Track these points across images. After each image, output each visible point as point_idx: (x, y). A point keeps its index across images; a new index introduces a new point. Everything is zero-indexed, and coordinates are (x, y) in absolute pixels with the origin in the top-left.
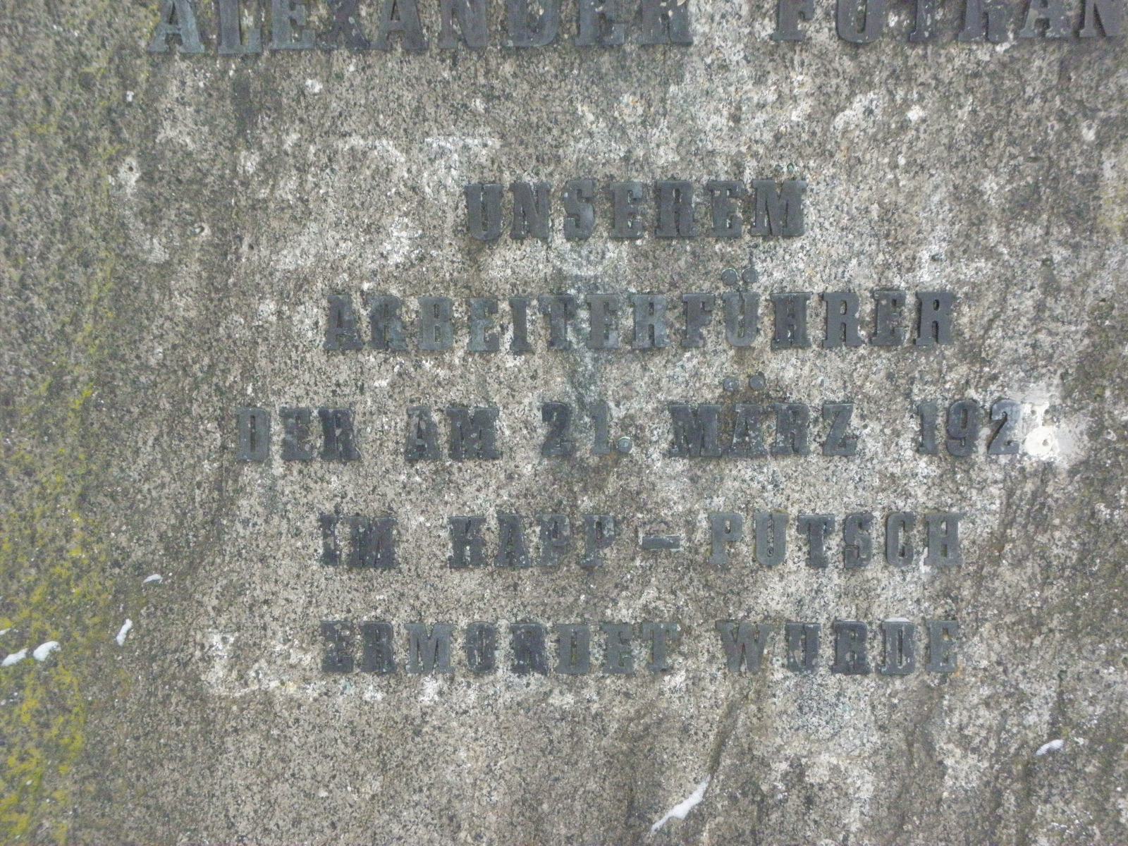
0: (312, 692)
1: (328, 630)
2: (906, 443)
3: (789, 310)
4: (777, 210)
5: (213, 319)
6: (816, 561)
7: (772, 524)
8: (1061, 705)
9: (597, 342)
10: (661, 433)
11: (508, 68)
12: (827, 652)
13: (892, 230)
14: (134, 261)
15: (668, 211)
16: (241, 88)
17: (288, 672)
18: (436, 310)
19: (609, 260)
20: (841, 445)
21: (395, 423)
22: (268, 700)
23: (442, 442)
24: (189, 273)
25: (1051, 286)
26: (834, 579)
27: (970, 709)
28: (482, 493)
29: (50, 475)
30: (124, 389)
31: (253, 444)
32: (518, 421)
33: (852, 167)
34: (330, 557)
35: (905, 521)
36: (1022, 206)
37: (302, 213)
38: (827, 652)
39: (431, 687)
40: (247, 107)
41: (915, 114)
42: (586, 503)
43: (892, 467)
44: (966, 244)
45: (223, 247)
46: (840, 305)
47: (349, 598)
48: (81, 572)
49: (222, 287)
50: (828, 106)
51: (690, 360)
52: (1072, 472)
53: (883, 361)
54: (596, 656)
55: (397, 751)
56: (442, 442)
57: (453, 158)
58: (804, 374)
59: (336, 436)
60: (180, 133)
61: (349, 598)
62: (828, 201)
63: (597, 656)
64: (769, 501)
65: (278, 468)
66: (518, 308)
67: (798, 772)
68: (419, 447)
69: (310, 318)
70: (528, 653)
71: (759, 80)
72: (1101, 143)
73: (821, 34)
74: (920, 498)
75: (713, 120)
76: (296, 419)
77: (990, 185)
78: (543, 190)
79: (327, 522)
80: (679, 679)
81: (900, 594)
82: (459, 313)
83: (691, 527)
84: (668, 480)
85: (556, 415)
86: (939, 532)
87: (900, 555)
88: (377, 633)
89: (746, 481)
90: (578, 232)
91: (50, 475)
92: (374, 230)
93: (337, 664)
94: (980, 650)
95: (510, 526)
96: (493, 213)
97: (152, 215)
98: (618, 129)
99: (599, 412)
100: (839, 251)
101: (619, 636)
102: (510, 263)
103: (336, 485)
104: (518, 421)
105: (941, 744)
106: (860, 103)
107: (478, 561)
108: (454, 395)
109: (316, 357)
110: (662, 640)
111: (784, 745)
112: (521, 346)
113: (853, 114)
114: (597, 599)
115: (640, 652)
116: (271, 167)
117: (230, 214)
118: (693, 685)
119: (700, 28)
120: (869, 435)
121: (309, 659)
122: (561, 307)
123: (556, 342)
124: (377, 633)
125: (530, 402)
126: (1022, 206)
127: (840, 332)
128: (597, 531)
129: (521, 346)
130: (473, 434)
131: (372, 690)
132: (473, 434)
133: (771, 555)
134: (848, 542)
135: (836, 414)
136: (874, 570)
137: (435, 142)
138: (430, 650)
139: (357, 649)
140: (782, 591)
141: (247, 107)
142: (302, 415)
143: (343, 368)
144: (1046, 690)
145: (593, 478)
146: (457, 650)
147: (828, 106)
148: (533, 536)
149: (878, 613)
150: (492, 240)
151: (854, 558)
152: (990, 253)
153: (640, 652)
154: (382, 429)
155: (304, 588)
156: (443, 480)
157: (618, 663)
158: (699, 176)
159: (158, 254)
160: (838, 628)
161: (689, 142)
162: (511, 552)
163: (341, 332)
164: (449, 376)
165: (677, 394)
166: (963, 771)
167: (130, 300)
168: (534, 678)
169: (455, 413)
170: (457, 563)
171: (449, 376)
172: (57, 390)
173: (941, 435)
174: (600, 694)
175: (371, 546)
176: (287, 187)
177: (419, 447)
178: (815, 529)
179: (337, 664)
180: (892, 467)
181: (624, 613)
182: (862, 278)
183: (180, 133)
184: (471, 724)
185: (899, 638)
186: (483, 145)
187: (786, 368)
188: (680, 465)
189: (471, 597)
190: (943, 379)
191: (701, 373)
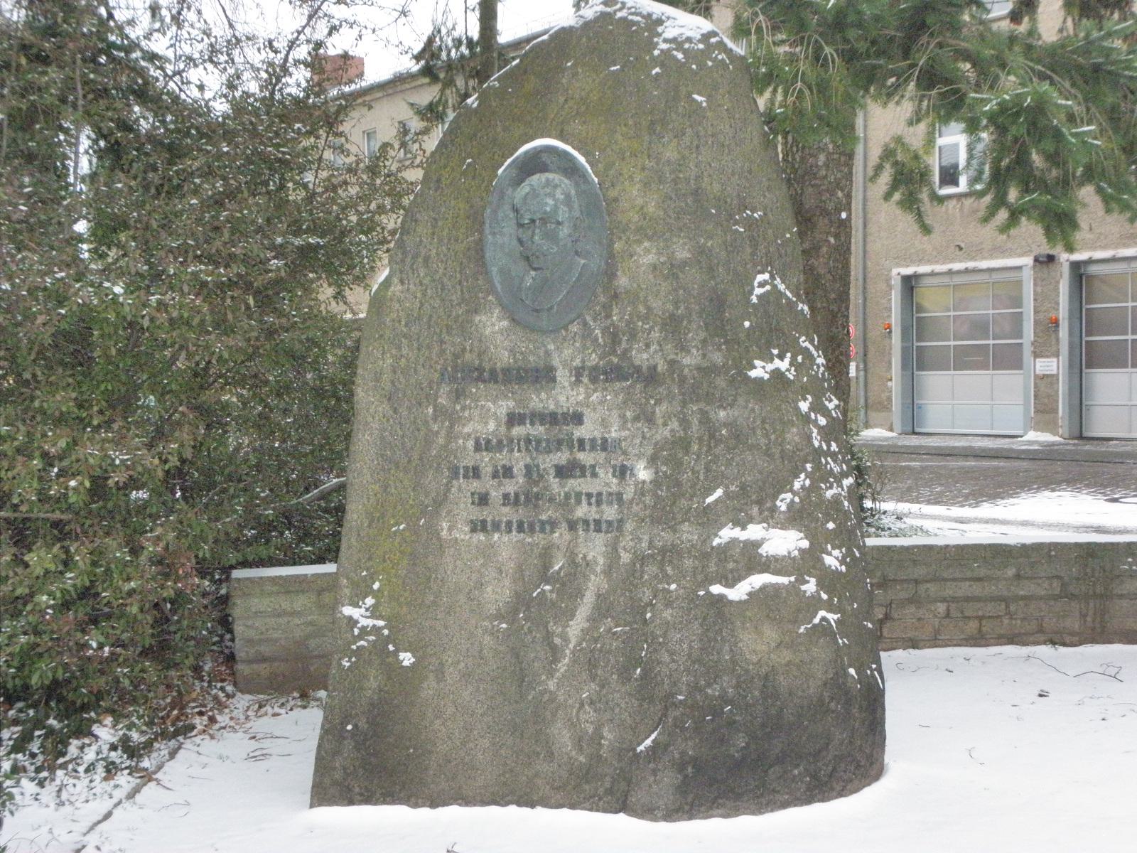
0: (467, 537)
1: (472, 521)
2: (610, 475)
3: (581, 442)
4: (578, 419)
5: (448, 443)
6: (590, 504)
7: (578, 495)
8: (651, 542)
9: (537, 449)
10: (552, 472)
11: (517, 387)
12: (592, 527)
13: (605, 423)
14: (431, 430)
15: (552, 419)
16: (457, 390)
17: (462, 533)
18: (500, 442)
19: (539, 430)
20: (594, 475)
21: (489, 469)
22: (456, 539)
23: (501, 474)
24: (443, 433)
25: (644, 438)
26: (594, 508)
27: (626, 541)
28: (510, 487)
29: (406, 482)
30: (426, 461)
31: (455, 474)
32: (519, 469)
33: (595, 409)
34: (473, 503)
35: (610, 494)
36: (636, 419)
37: (470, 419)
38: (592, 527)
39: (496, 536)
40: (458, 395)
41: (608, 398)
42: (535, 490)
43: (606, 480)
44: (623, 427)
45: (451, 426)
46: (593, 440)
47: (477, 513)
48: (412, 506)
49: (451, 436)
50: (588, 396)
51: (559, 454)
52: (651, 482)
53: (603, 455)
54: (537, 529)
55: (488, 552)
56: (501, 474)
57: (504, 407)
58: (585, 458)
59: (475, 472)
60: (442, 401)
61: (477, 513)
62: (590, 418)
63: (537, 529)
64: (578, 489)
65: (461, 480)
66: (519, 441)
67: (585, 557)
68: (495, 475)
69: (470, 444)
70: (520, 529)
71: (572, 390)
72: (655, 404)
73: (585, 380)
74: (614, 488)
75: (562, 399)
76: (466, 468)
77: (628, 414)
78: (525, 414)
79: (472, 494)
80: (557, 534)
81: (610, 513)
82: (505, 442)
83: (560, 495)
84: (554, 482)
85: (527, 467)
86: (619, 496)
87: (610, 503)
88: (484, 522)
89: (574, 484)
90: (532, 424)
91: (406, 482)
92: (486, 423)
93: (473, 530)
94: (629, 526)
95: (517, 495)
96: (513, 419)
97: (435, 419)
98: (541, 401)
99: (538, 466)
100: (592, 429)
101: (543, 523)
102: (517, 431)
103: (475, 485)
104: (519, 469)
105: (620, 550)
106: (595, 395)
107: (509, 504)
108: (504, 462)
109: (471, 453)
110: (553, 524)
111: (581, 550)
112: (519, 451)
113: (594, 397)
114: (536, 515)
115: (548, 527)
116: (463, 408)
117: (454, 419)
118: (560, 536)
119: (559, 379)
120: (601, 472)
121: (467, 529)
122: (528, 441)
123: (527, 449)
124: (484, 522)
125: (522, 464)
126: (636, 419)
127: (593, 448)
128: (538, 497)
129: (519, 451)
130: (508, 472)
131: (482, 537)
132: (508, 472)
133: (579, 502)
134: (598, 499)
135: (593, 467)
136: (604, 507)
137: (500, 403)
138: (496, 526)
139: (479, 526)
140: (581, 511)
141: (458, 395)
142: (468, 467)
143: (478, 456)
144: (646, 537)
145: (536, 483)
146: (503, 527)
147: (588, 396)
148: (522, 498)
149: (605, 517)
150: (513, 425)
151: (599, 503)
152: (629, 430)
153: (548, 527)
154: (487, 470)
155: (465, 510)
156: (500, 484)
157: (543, 530)
158: (560, 411)
159: (436, 429)
160: (595, 520)
161: (557, 403)
162: (516, 502)
163: (478, 448)
164: (502, 458)
165: (556, 462)
166: (625, 557)
167: (428, 442)
168: (522, 535)
169: (504, 466)
170: (504, 504)
171: (502, 458)
172: (409, 462)
173: (617, 473)
174: (539, 538)
175: (483, 500)
176: (467, 414)
177: (495, 475)
178: (589, 495)
179: (473, 530)
180: (606, 480)
181: (544, 517)
182: (597, 434)
183: (442, 401)
184: (506, 545)
185: (609, 523)
186: (511, 404)
187: (582, 456)
188: (557, 480)
189: (507, 513)
190: (618, 460)
191: (562, 457)
